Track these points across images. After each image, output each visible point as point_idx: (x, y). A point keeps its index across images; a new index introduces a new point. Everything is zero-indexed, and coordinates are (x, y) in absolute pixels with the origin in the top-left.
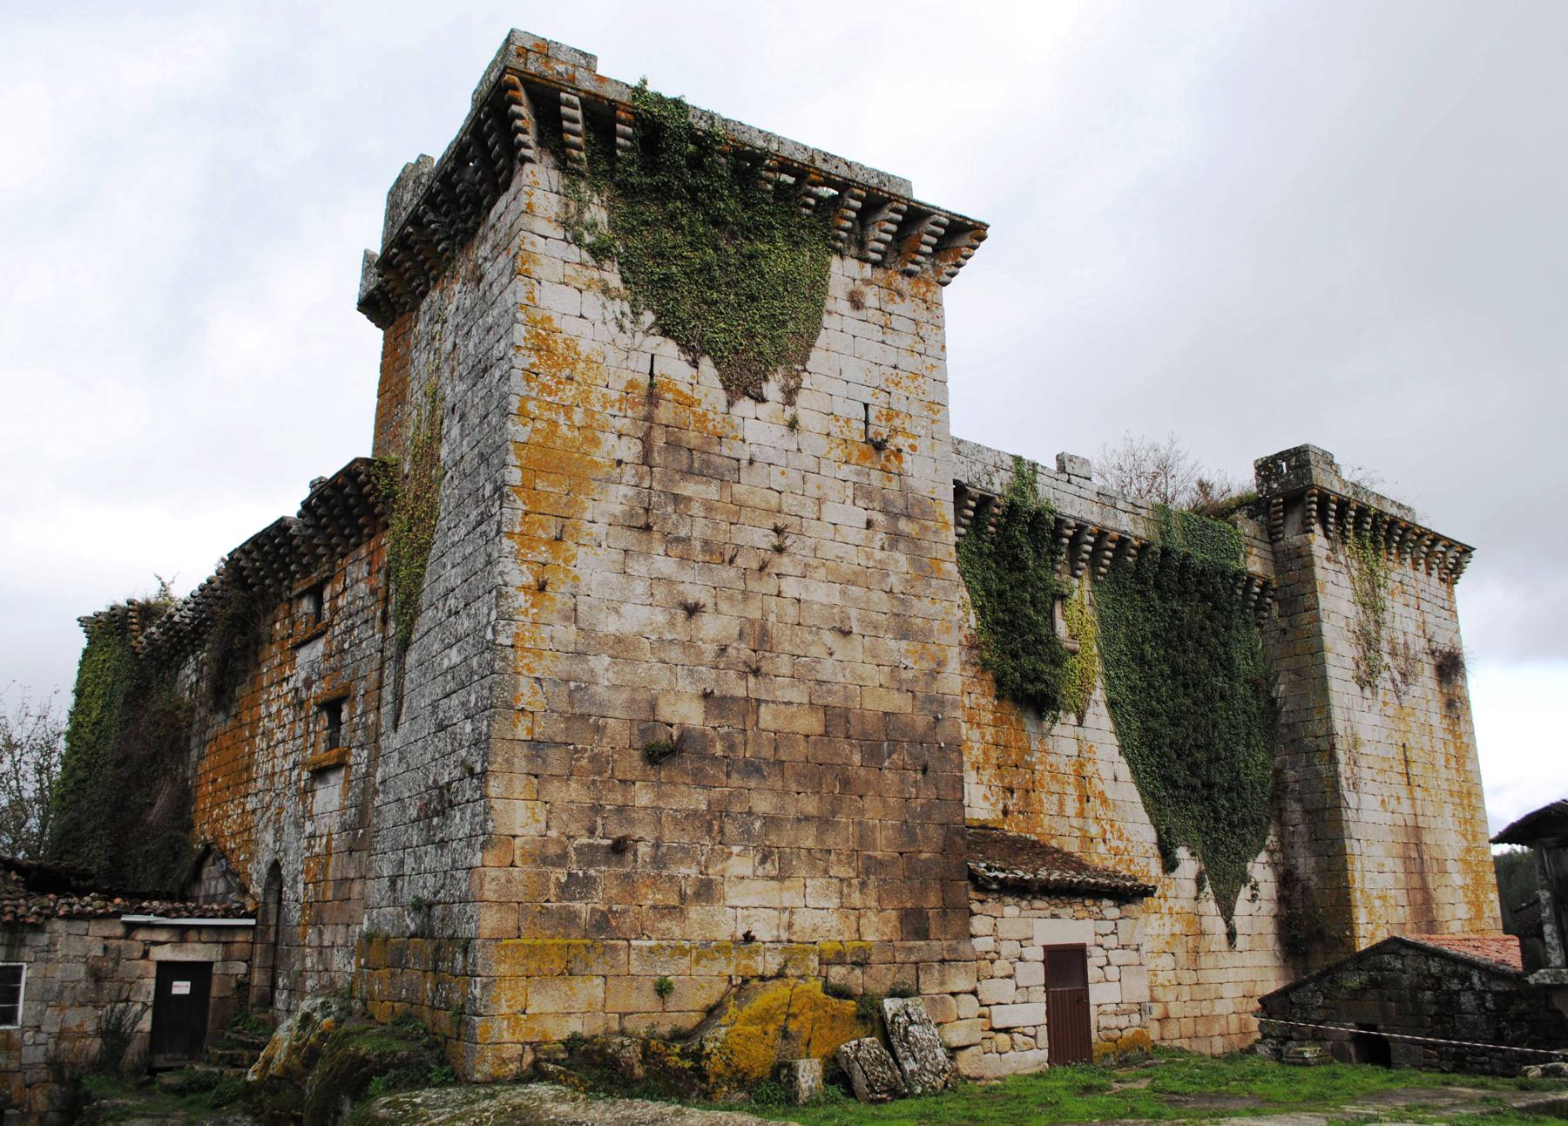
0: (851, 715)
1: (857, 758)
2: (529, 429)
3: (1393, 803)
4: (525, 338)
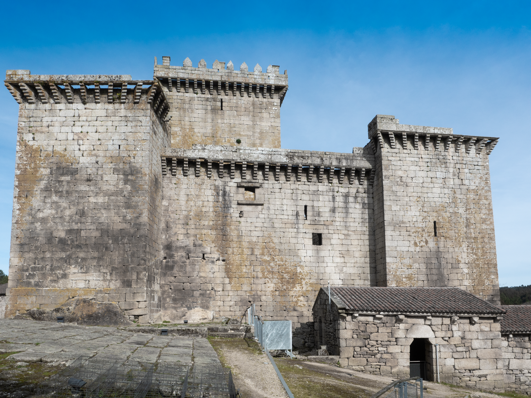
1: (110, 242)
3: (423, 244)
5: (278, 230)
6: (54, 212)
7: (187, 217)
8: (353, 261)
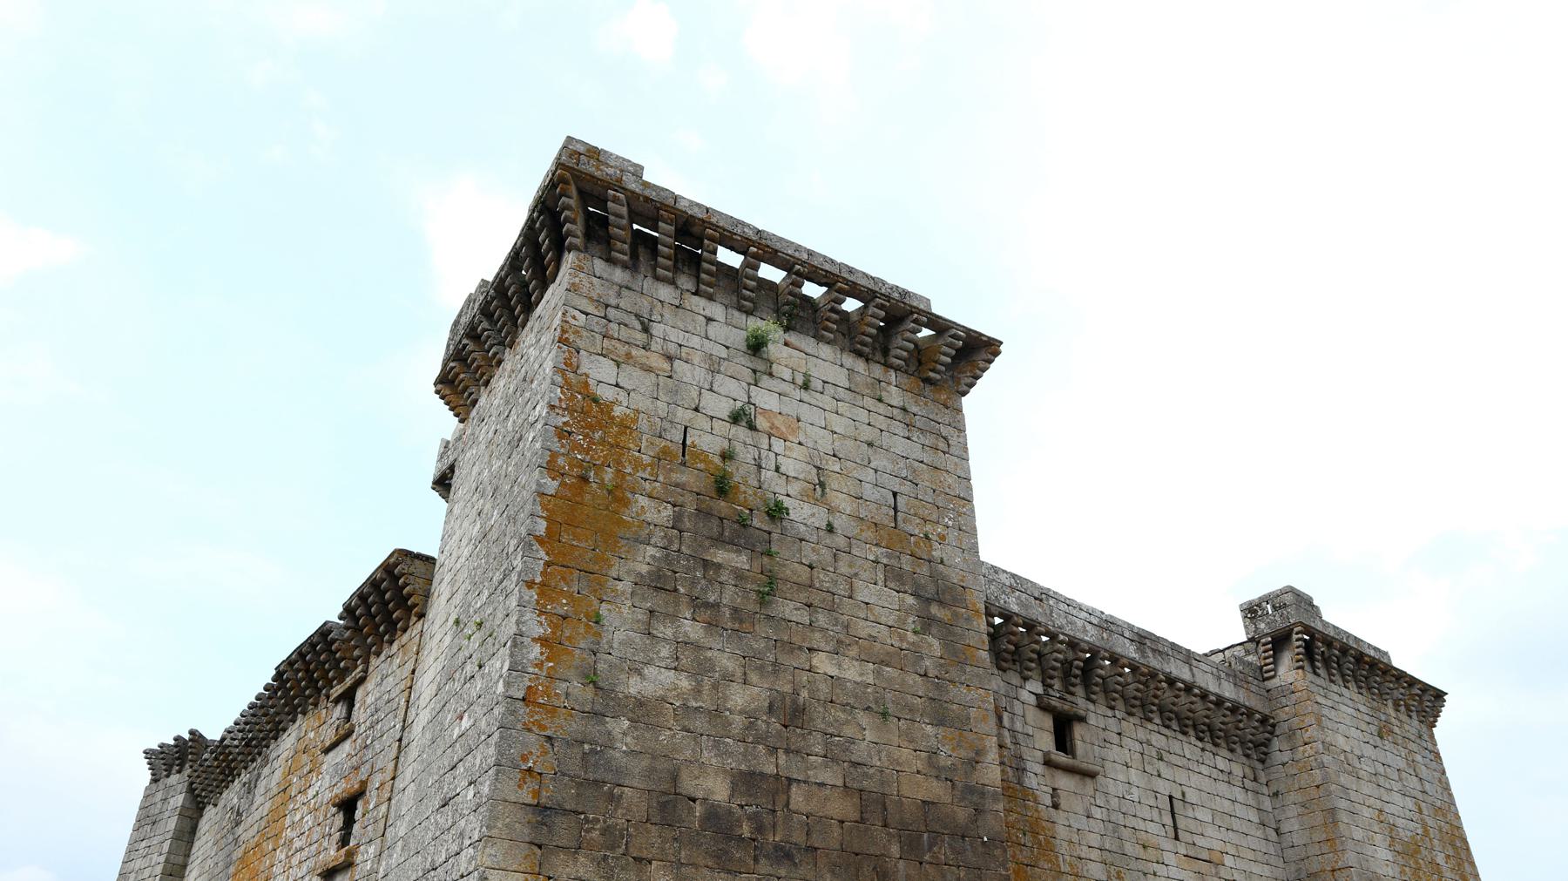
0: (888, 802)
1: (895, 850)
2: (556, 484)
4: (560, 400)
6: (685, 683)
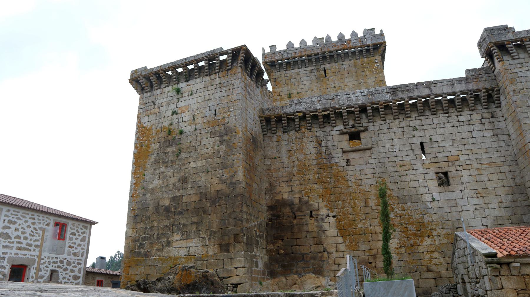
0: (207, 194)
1: (208, 205)
5: (393, 174)
7: (290, 174)
8: (496, 201)
